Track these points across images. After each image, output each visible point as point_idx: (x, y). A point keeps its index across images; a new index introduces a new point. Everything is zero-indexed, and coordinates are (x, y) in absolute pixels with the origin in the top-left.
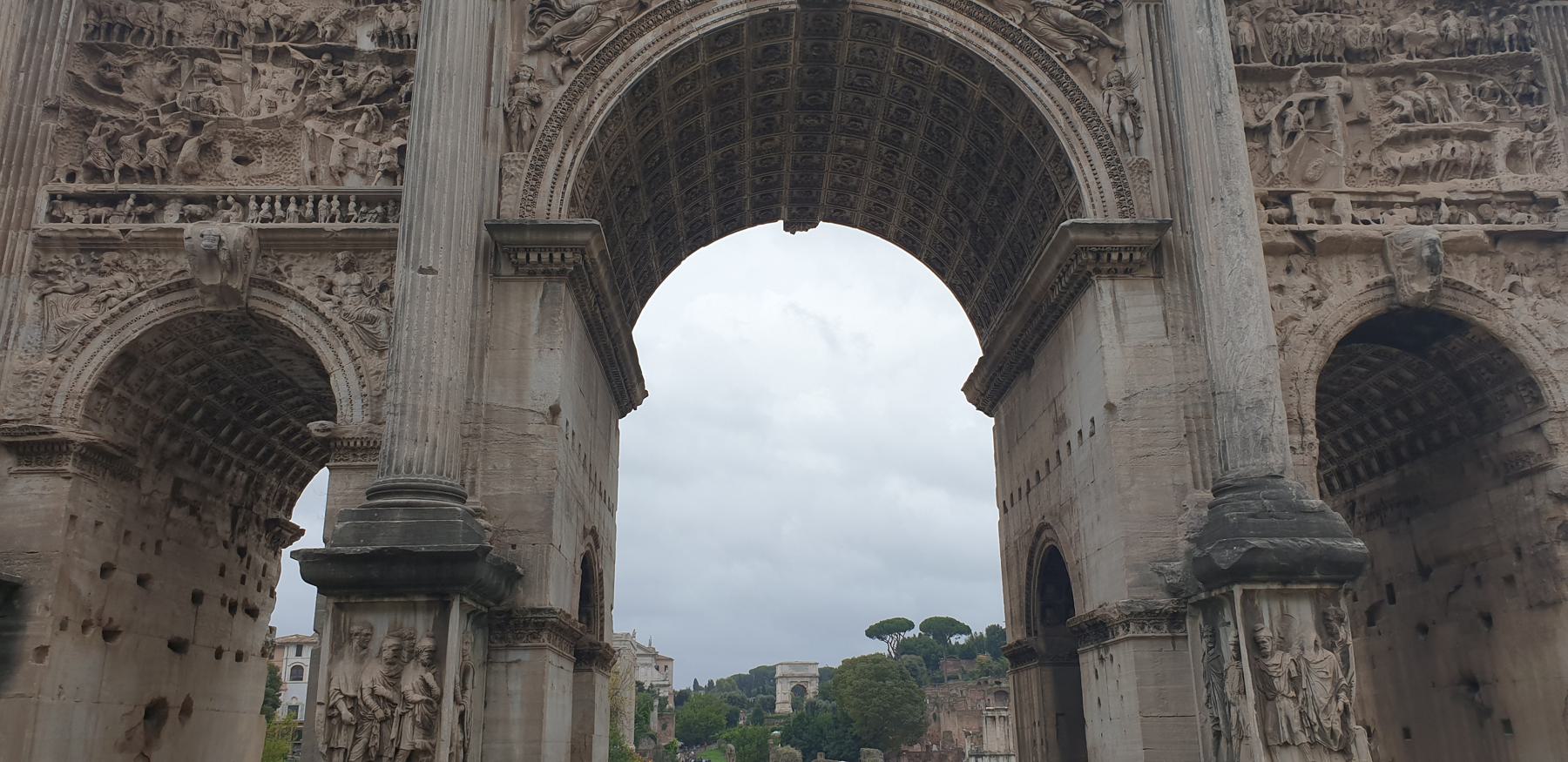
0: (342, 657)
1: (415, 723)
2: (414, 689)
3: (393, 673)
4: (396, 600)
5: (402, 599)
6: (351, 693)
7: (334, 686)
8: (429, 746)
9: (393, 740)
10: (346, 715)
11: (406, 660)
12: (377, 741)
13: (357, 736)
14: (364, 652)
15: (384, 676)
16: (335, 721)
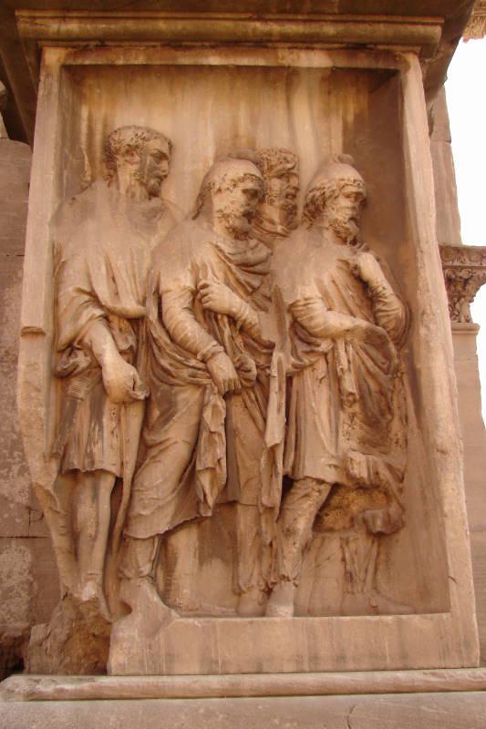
0: (87, 211)
1: (341, 400)
2: (326, 297)
3: (251, 256)
4: (245, 61)
5: (260, 61)
6: (130, 305)
7: (74, 280)
8: (385, 474)
9: (273, 449)
10: (117, 371)
11: (279, 229)
12: (220, 452)
13: (150, 438)
14: (155, 202)
15: (225, 258)
16: (80, 388)
